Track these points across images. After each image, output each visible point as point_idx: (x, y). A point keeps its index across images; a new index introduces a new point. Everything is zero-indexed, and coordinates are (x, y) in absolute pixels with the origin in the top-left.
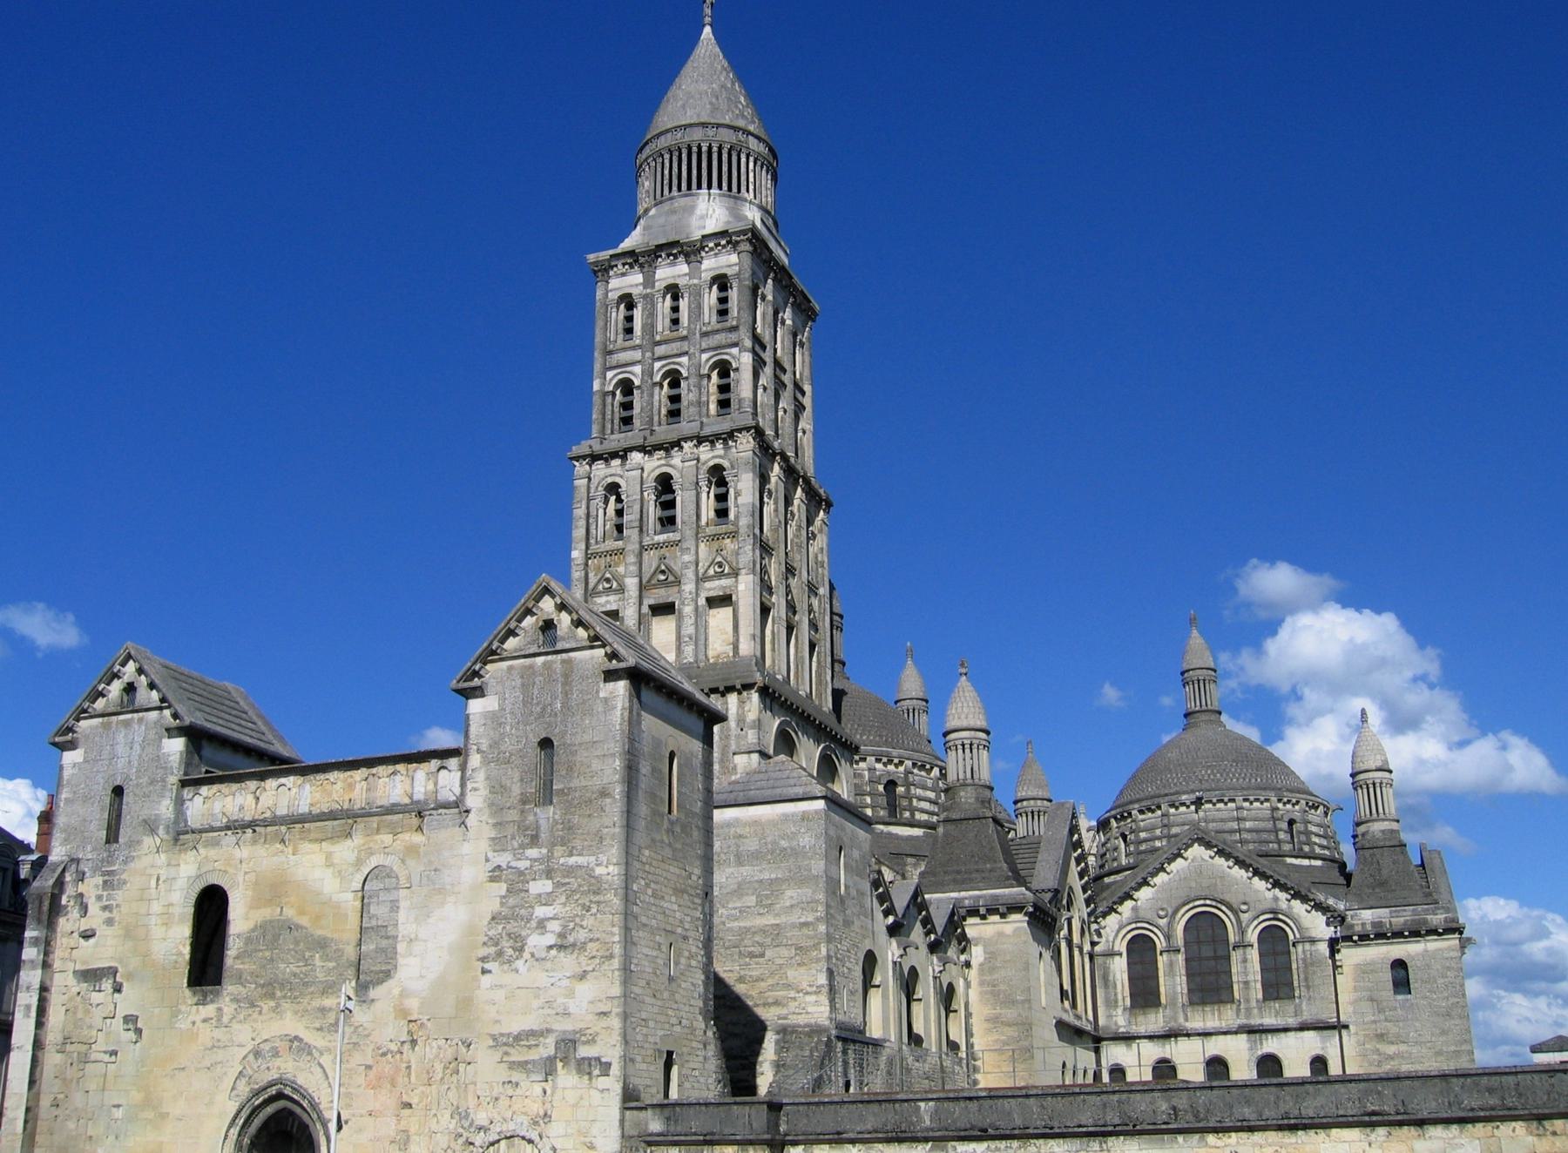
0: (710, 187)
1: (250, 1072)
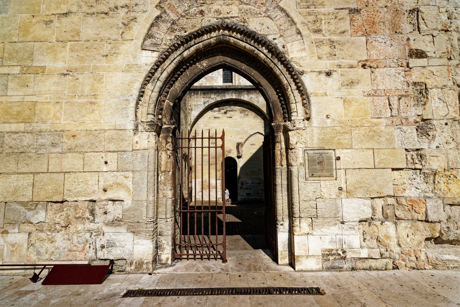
1: (173, 16)
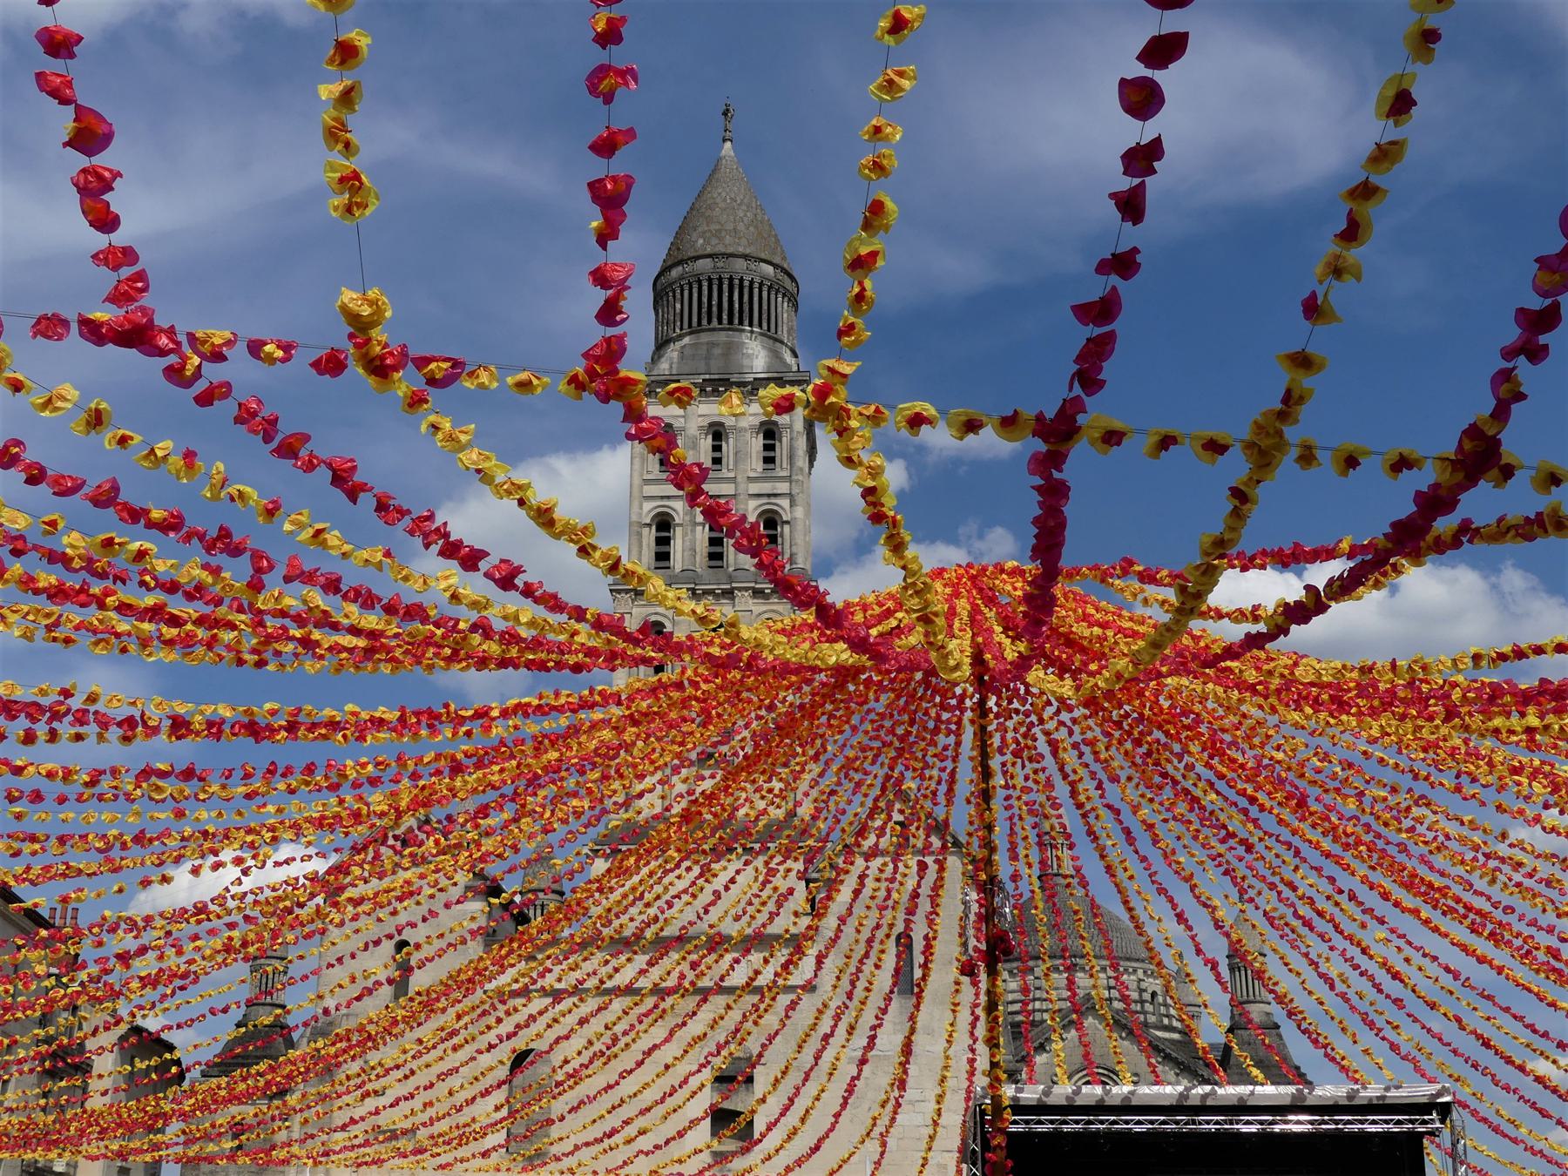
0: (751, 325)
